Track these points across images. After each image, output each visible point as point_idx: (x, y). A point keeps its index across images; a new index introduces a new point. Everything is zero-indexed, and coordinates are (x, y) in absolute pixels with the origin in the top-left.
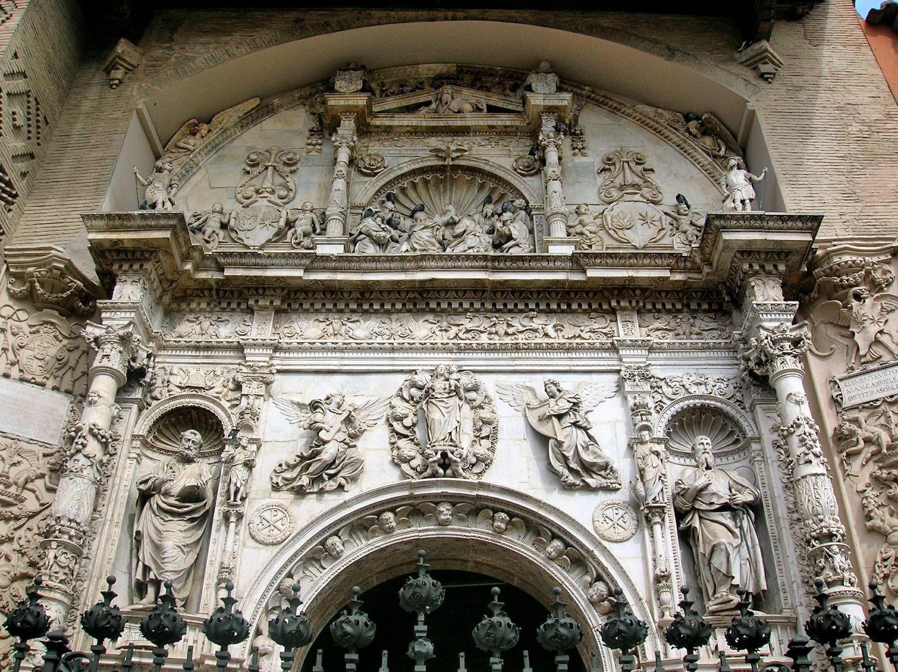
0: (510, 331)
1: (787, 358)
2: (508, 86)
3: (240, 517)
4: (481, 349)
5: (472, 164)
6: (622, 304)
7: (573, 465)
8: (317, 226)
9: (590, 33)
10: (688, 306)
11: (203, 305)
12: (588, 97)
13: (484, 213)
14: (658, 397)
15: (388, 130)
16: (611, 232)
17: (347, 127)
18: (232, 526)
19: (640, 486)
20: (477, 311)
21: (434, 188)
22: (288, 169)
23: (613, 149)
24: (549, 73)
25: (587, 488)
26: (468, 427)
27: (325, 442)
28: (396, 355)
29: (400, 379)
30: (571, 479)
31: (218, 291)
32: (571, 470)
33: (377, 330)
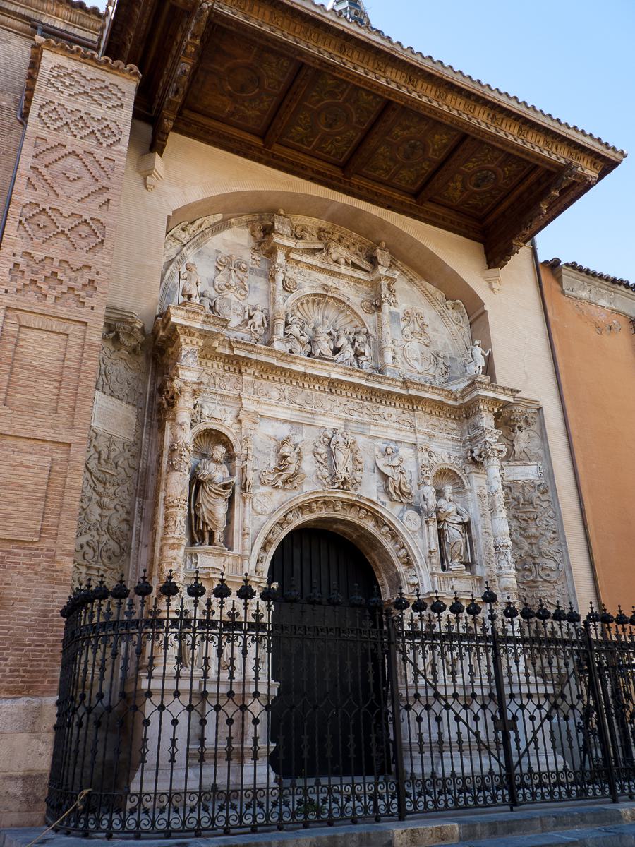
5: (340, 298)
8: (265, 322)
15: (298, 262)
17: (281, 258)
30: (395, 497)
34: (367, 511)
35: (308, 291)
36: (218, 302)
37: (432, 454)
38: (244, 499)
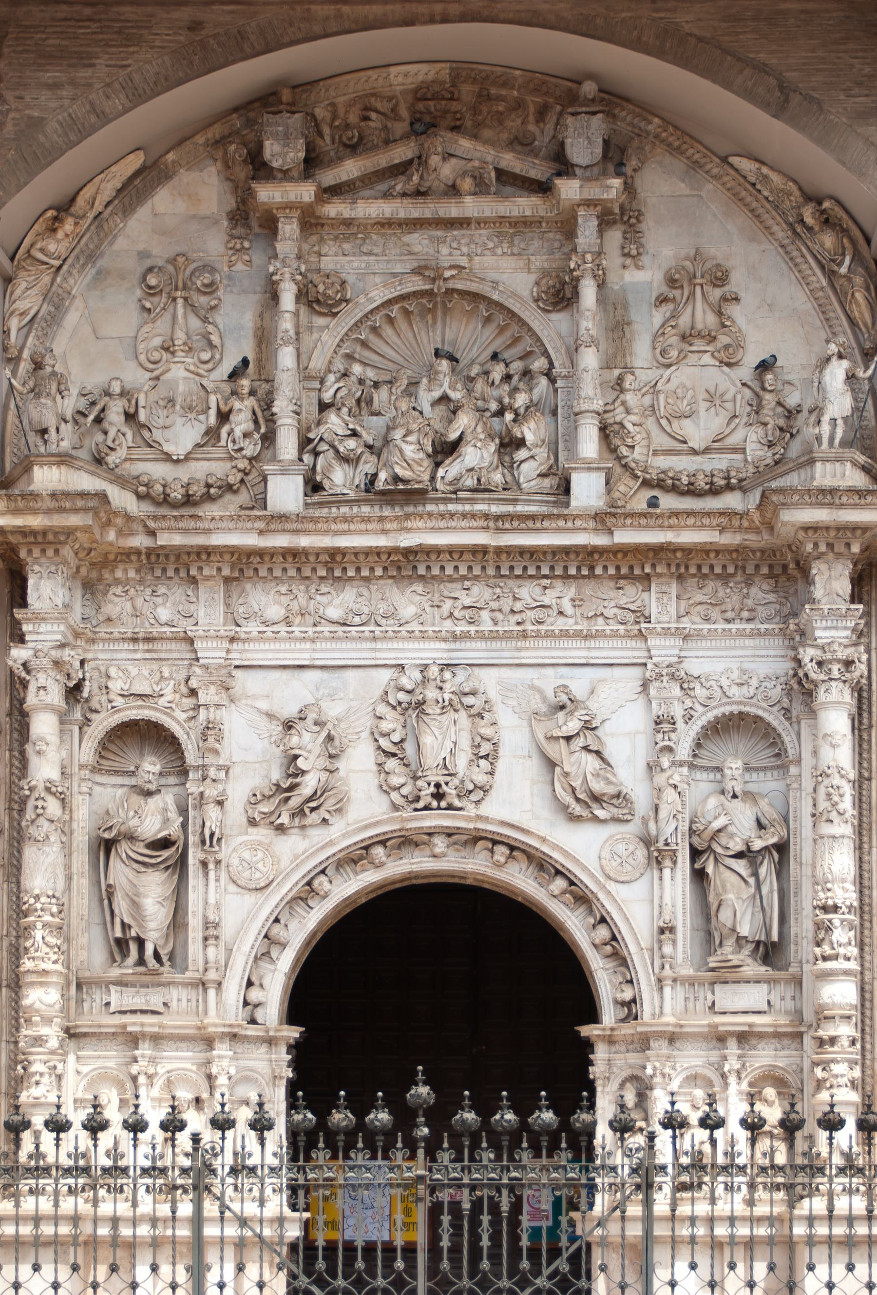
0: (518, 606)
1: (833, 684)
2: (532, 109)
3: (218, 862)
4: (481, 636)
5: (473, 287)
6: (659, 569)
7: (582, 796)
8: (261, 421)
9: (659, 53)
10: (744, 568)
11: (132, 574)
12: (657, 136)
13: (490, 381)
14: (688, 703)
15: (348, 223)
16: (664, 422)
18: (212, 874)
19: (652, 826)
20: (476, 578)
21: (418, 319)
22: (203, 300)
23: (683, 253)
24: (594, 113)
25: (596, 819)
26: (465, 743)
27: (303, 772)
28: (379, 645)
29: (385, 675)
30: (578, 809)
31: (148, 555)
32: (578, 800)
33: (355, 607)
34: (512, 848)
35: (379, 296)
36: (142, 403)
37: (685, 684)
38: (204, 864)
